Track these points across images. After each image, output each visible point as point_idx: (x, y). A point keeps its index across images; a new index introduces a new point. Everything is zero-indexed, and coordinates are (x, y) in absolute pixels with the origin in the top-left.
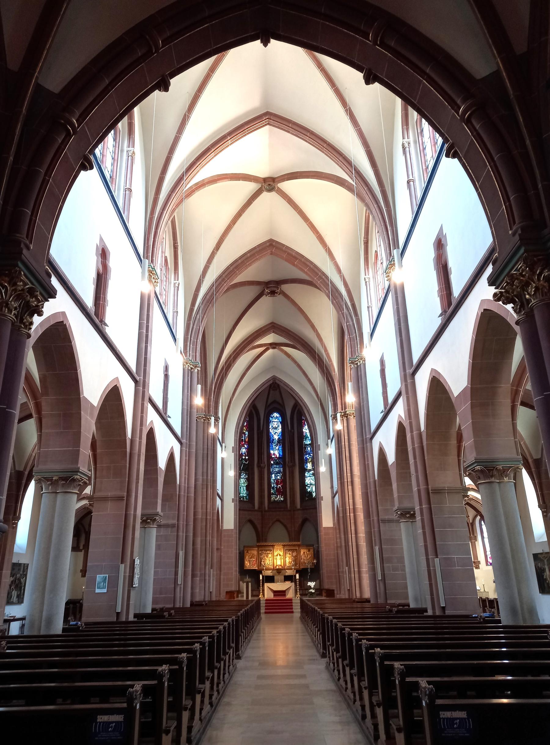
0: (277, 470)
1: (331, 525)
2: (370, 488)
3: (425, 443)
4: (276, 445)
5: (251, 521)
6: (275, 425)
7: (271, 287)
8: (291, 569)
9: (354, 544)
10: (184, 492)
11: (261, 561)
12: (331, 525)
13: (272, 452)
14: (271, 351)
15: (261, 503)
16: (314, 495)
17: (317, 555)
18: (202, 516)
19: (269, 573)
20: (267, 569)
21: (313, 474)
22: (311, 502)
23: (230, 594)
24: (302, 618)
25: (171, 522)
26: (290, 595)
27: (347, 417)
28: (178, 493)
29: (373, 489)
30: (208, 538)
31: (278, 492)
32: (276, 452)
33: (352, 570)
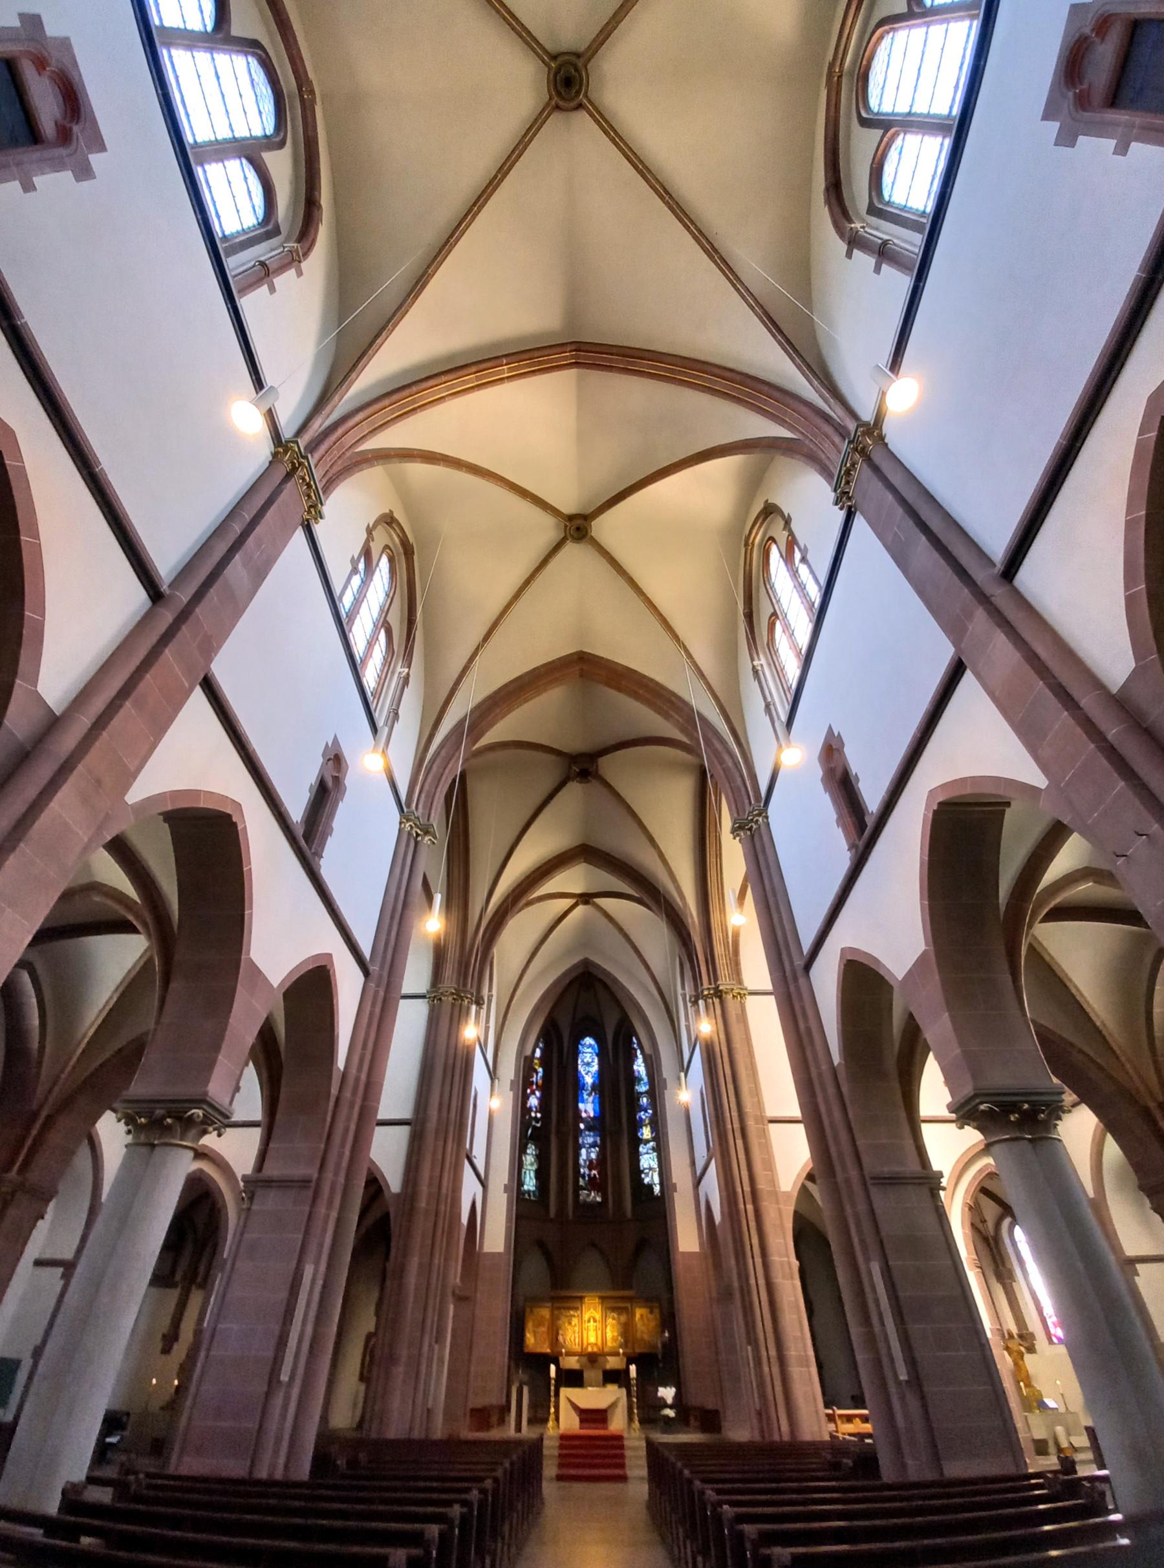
0: (590, 1140)
1: (695, 1248)
2: (824, 1090)
3: (845, 1089)
4: (589, 1095)
5: (541, 1245)
6: (588, 1058)
7: (582, 766)
8: (618, 1354)
9: (762, 1282)
10: (354, 1093)
11: (558, 1334)
12: (695, 1248)
13: (581, 1106)
14: (581, 909)
15: (562, 1203)
16: (657, 1189)
17: (669, 1319)
18: (428, 1204)
19: (571, 1363)
20: (569, 1354)
21: (653, 1149)
22: (653, 1210)
23: (482, 1417)
24: (653, 1505)
25: (299, 1171)
26: (618, 1423)
27: (720, 997)
28: (334, 1091)
29: (831, 1090)
30: (436, 1261)
31: (593, 1184)
32: (588, 1107)
33: (764, 1353)
